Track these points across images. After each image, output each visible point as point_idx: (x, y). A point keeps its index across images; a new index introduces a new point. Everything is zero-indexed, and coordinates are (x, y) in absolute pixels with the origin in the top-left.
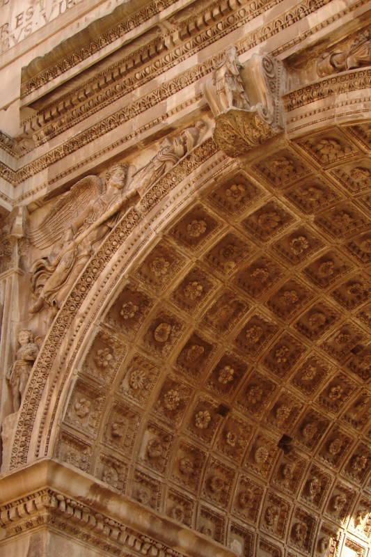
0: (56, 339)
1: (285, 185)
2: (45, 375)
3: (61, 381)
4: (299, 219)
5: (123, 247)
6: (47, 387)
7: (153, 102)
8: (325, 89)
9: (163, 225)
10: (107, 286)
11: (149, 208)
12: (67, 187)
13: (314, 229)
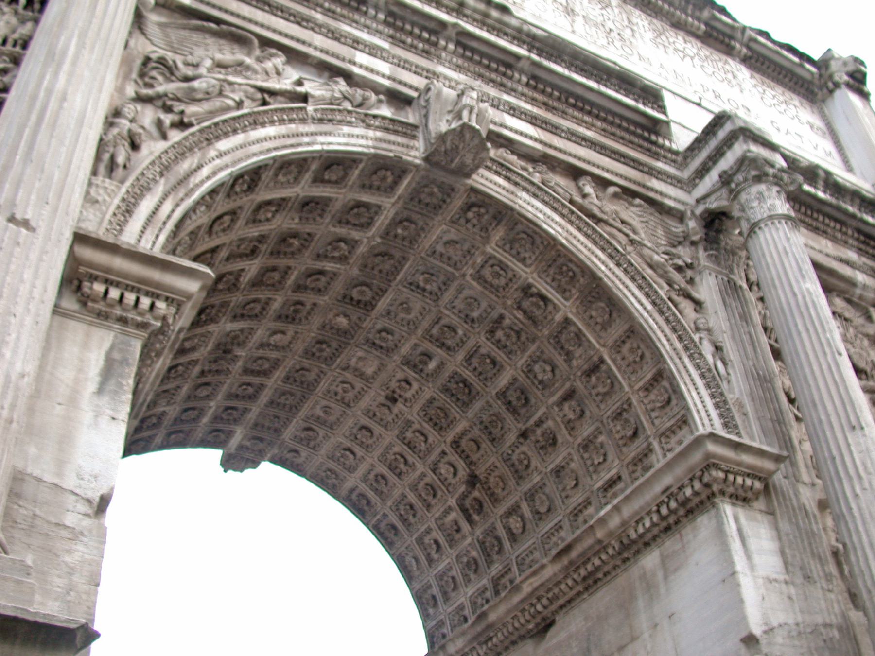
0: (182, 152)
1: (410, 206)
2: (162, 175)
4: (370, 234)
5: (282, 129)
7: (343, 40)
8: (514, 177)
9: (331, 147)
10: (255, 148)
11: (321, 121)
12: (218, 21)
13: (362, 249)
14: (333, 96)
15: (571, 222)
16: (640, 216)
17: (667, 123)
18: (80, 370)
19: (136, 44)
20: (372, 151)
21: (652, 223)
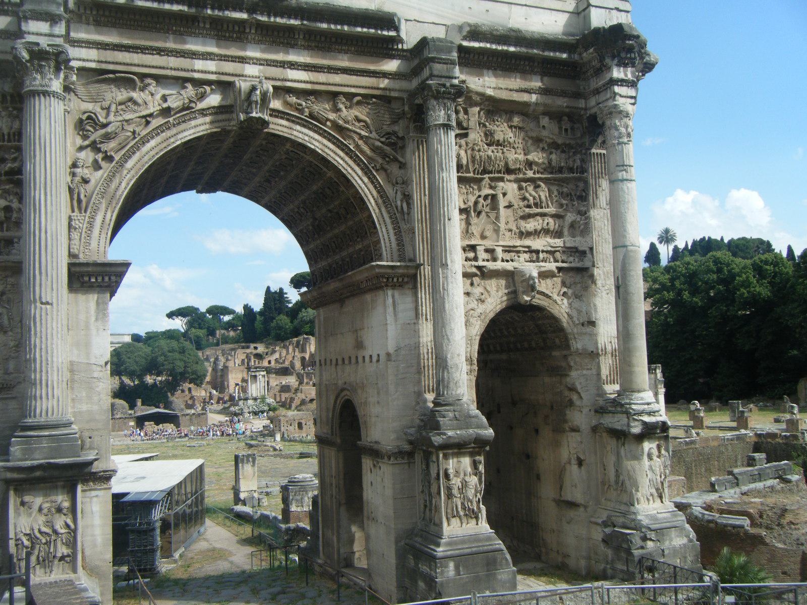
3: (114, 205)
5: (158, 139)
6: (103, 206)
7: (186, 56)
10: (146, 158)
11: (179, 124)
14: (184, 104)
15: (325, 137)
16: (374, 110)
17: (399, 36)
18: (87, 312)
19: (74, 106)
20: (209, 131)
21: (382, 112)
